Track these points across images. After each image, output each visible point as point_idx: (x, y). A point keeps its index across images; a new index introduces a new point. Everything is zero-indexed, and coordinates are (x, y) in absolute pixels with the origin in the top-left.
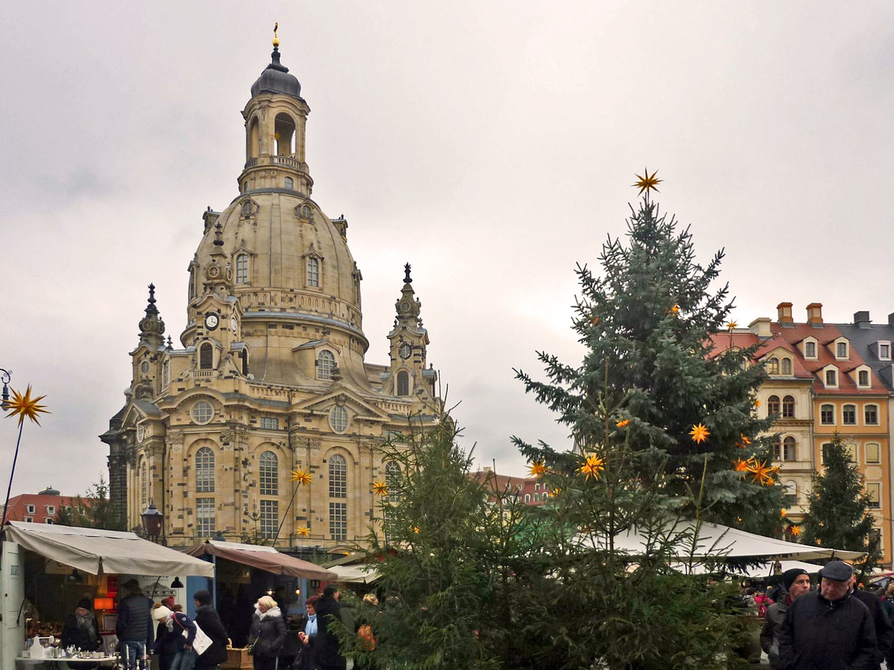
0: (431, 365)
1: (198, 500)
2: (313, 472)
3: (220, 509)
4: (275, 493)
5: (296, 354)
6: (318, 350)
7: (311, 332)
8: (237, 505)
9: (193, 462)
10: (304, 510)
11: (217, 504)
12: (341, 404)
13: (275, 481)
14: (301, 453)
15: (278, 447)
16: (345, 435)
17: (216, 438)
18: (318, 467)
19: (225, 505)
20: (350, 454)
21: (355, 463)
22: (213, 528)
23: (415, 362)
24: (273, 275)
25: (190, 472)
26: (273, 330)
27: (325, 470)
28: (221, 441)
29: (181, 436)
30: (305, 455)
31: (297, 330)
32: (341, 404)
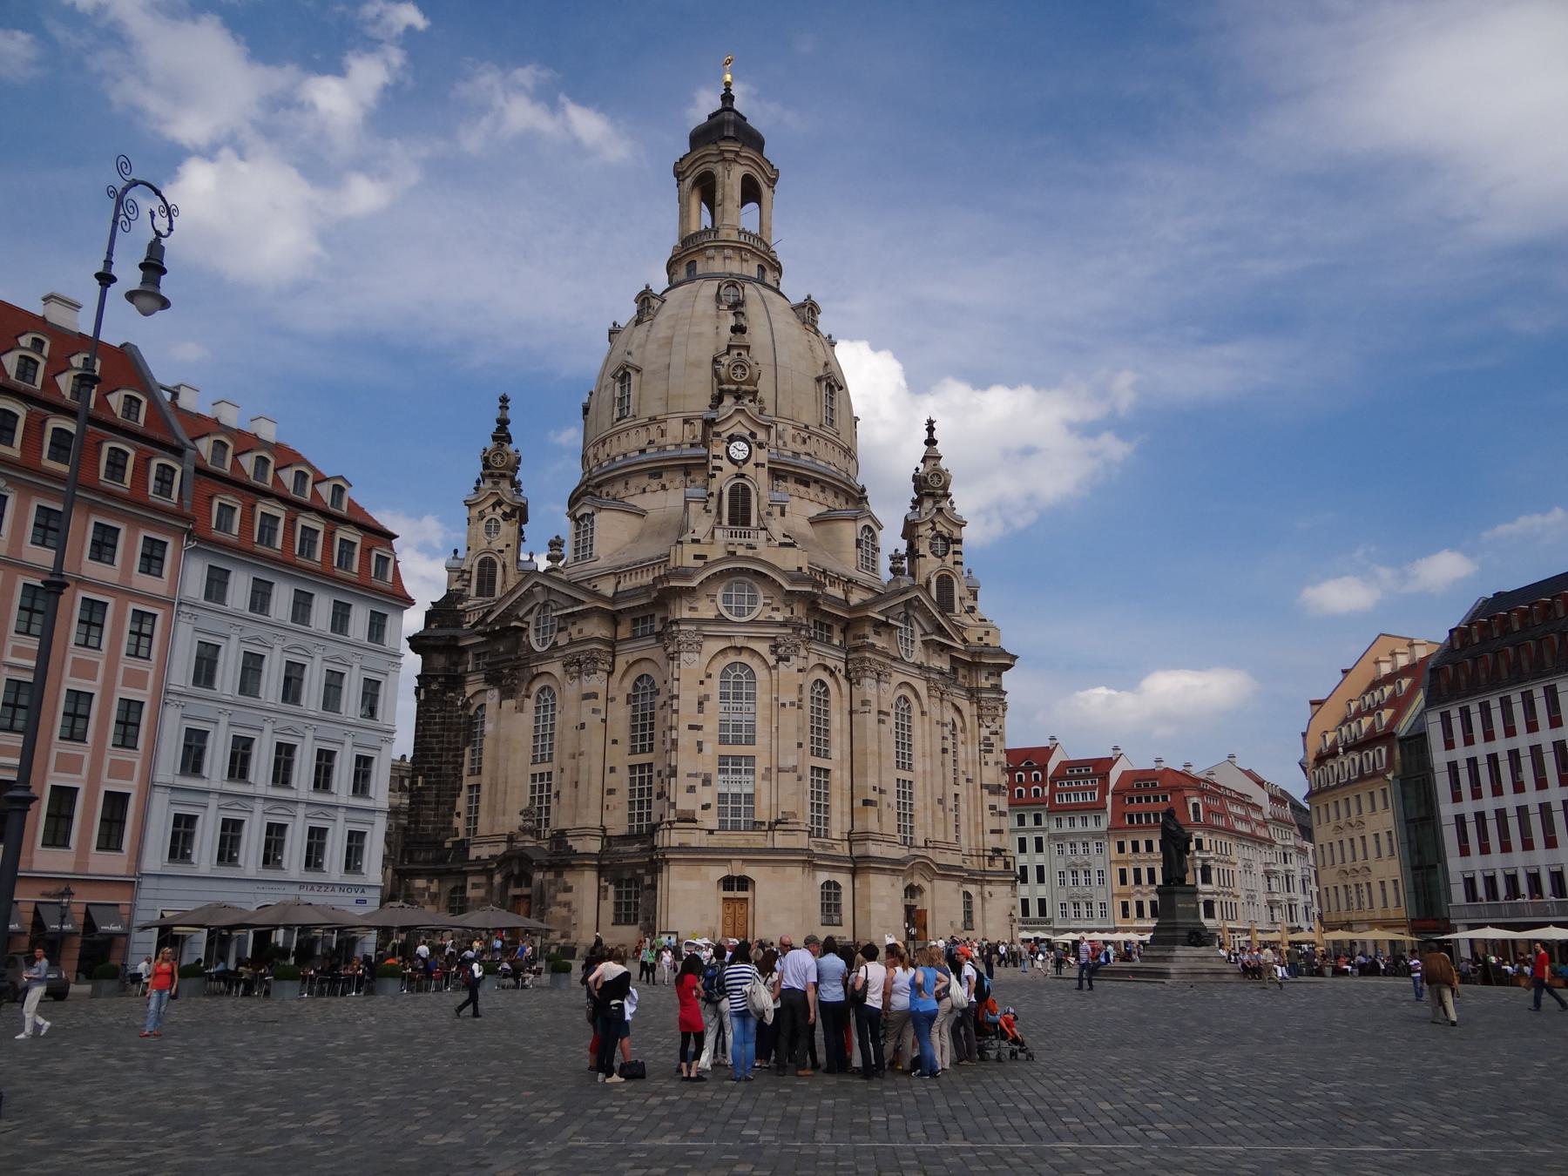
1: (723, 759)
3: (763, 778)
5: (821, 528)
6: (861, 524)
9: (714, 687)
11: (761, 765)
12: (911, 612)
14: (869, 687)
15: (832, 673)
18: (887, 714)
19: (779, 770)
20: (917, 696)
23: (956, 563)
27: (891, 721)
28: (773, 652)
30: (874, 691)
31: (813, 490)
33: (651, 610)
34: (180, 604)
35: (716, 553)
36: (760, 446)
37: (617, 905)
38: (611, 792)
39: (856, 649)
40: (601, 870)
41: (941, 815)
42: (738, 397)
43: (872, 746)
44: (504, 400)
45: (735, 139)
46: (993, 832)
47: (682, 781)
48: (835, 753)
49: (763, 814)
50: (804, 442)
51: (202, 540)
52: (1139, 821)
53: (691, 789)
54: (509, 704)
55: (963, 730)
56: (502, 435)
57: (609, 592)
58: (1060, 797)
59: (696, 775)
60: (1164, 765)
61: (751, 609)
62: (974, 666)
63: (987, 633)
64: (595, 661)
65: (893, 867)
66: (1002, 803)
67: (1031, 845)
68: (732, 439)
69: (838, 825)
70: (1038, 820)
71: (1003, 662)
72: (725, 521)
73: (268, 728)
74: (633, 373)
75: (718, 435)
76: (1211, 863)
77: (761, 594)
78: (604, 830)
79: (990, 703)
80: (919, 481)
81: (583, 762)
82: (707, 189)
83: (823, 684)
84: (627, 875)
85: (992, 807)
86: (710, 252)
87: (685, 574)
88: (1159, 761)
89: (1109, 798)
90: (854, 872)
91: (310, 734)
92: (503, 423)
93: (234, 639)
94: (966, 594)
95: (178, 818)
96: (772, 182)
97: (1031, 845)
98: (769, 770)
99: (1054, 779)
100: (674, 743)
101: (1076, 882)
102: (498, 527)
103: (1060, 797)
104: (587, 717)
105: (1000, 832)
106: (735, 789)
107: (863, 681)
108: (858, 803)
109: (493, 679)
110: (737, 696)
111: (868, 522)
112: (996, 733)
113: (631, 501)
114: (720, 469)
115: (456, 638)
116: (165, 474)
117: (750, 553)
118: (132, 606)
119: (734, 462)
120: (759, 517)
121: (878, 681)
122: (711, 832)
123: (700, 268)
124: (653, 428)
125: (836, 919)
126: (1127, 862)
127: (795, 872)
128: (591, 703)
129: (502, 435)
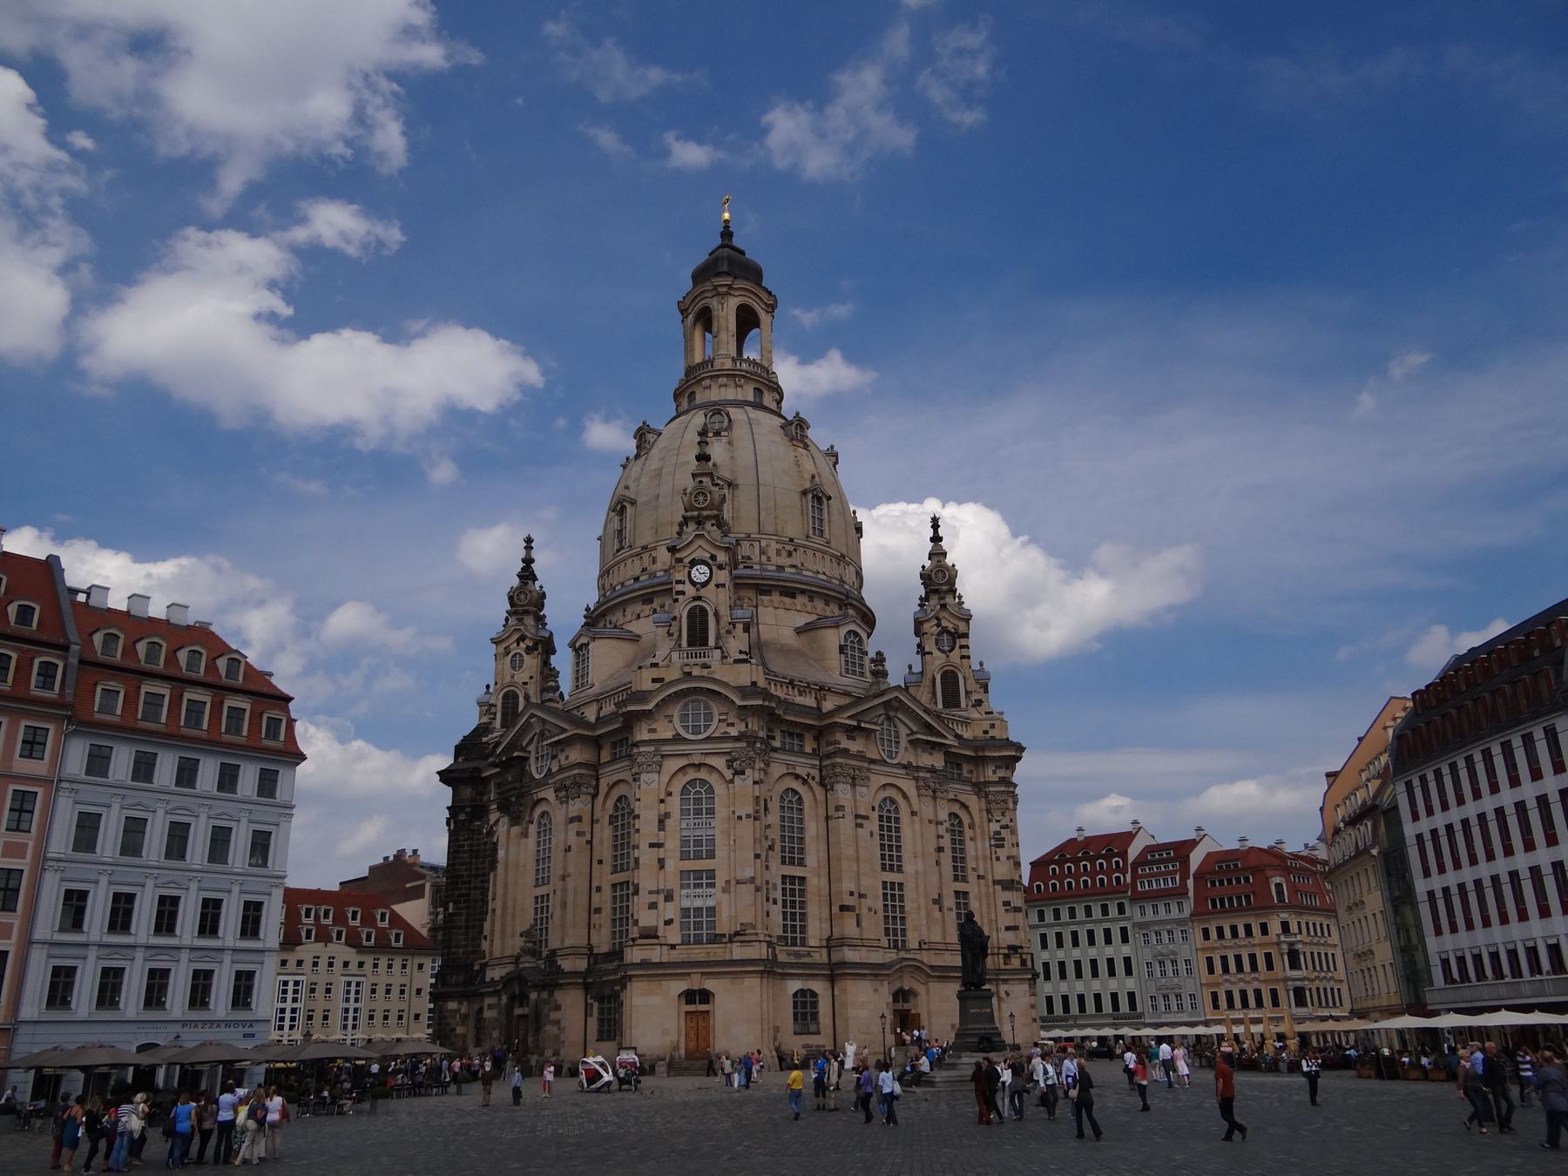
0: (981, 664)
1: (684, 874)
2: (861, 826)
3: (725, 890)
4: (801, 863)
5: (805, 637)
6: (844, 630)
7: (819, 605)
8: (758, 882)
9: (674, 804)
10: (852, 894)
11: (720, 881)
12: (892, 714)
13: (801, 840)
14: (843, 793)
15: (805, 782)
16: (899, 765)
17: (719, 762)
18: (867, 818)
19: (738, 882)
20: (905, 796)
21: (913, 813)
22: (712, 925)
23: (963, 657)
24: (763, 514)
25: (668, 822)
26: (765, 598)
27: (873, 824)
29: (658, 758)
30: (849, 796)
31: (801, 600)
32: (892, 714)
33: (615, 733)
34: (60, 781)
35: (675, 674)
36: (720, 567)
37: (601, 1021)
38: (598, 910)
39: (829, 756)
40: (587, 987)
41: (937, 914)
42: (700, 522)
43: (848, 851)
44: (529, 541)
45: (728, 274)
46: (1008, 929)
47: (643, 898)
48: (811, 860)
49: (724, 927)
50: (790, 554)
51: (81, 723)
52: (1222, 905)
53: (653, 906)
54: (516, 830)
55: (972, 826)
56: (527, 574)
57: (592, 718)
58: (1142, 883)
59: (658, 892)
60: (1249, 844)
61: (707, 727)
62: (979, 761)
63: (993, 726)
64: (579, 786)
65: (875, 972)
66: (1017, 899)
67: (1052, 941)
68: (693, 563)
69: (816, 931)
70: (1121, 909)
71: (1011, 754)
72: (684, 643)
73: (150, 883)
74: (630, 510)
75: (680, 560)
76: (1299, 947)
77: (716, 712)
78: (591, 948)
79: (1003, 797)
80: (926, 577)
81: (570, 883)
82: (705, 319)
83: (795, 792)
84: (607, 992)
85: (1006, 903)
86: (706, 383)
87: (643, 696)
88: (1243, 840)
89: (1190, 883)
90: (832, 979)
91: (194, 886)
92: (528, 561)
93: (116, 808)
94: (972, 685)
95: (57, 971)
96: (771, 309)
97: (1116, 936)
98: (728, 882)
99: (1136, 864)
100: (637, 860)
101: (1163, 973)
102: (522, 661)
103: (1142, 883)
104: (573, 840)
105: (1015, 928)
106: (698, 903)
107: (836, 787)
108: (835, 909)
109: (503, 808)
110: (698, 812)
111: (853, 627)
112: (1006, 827)
113: (628, 627)
114: (683, 593)
115: (479, 770)
116: (47, 671)
117: (705, 672)
118: (12, 787)
119: (693, 583)
120: (718, 637)
121: (853, 785)
122: (673, 947)
123: (699, 399)
124: (646, 556)
125: (813, 1028)
126: (1213, 949)
127: (753, 983)
128: (574, 827)
129: (527, 574)
